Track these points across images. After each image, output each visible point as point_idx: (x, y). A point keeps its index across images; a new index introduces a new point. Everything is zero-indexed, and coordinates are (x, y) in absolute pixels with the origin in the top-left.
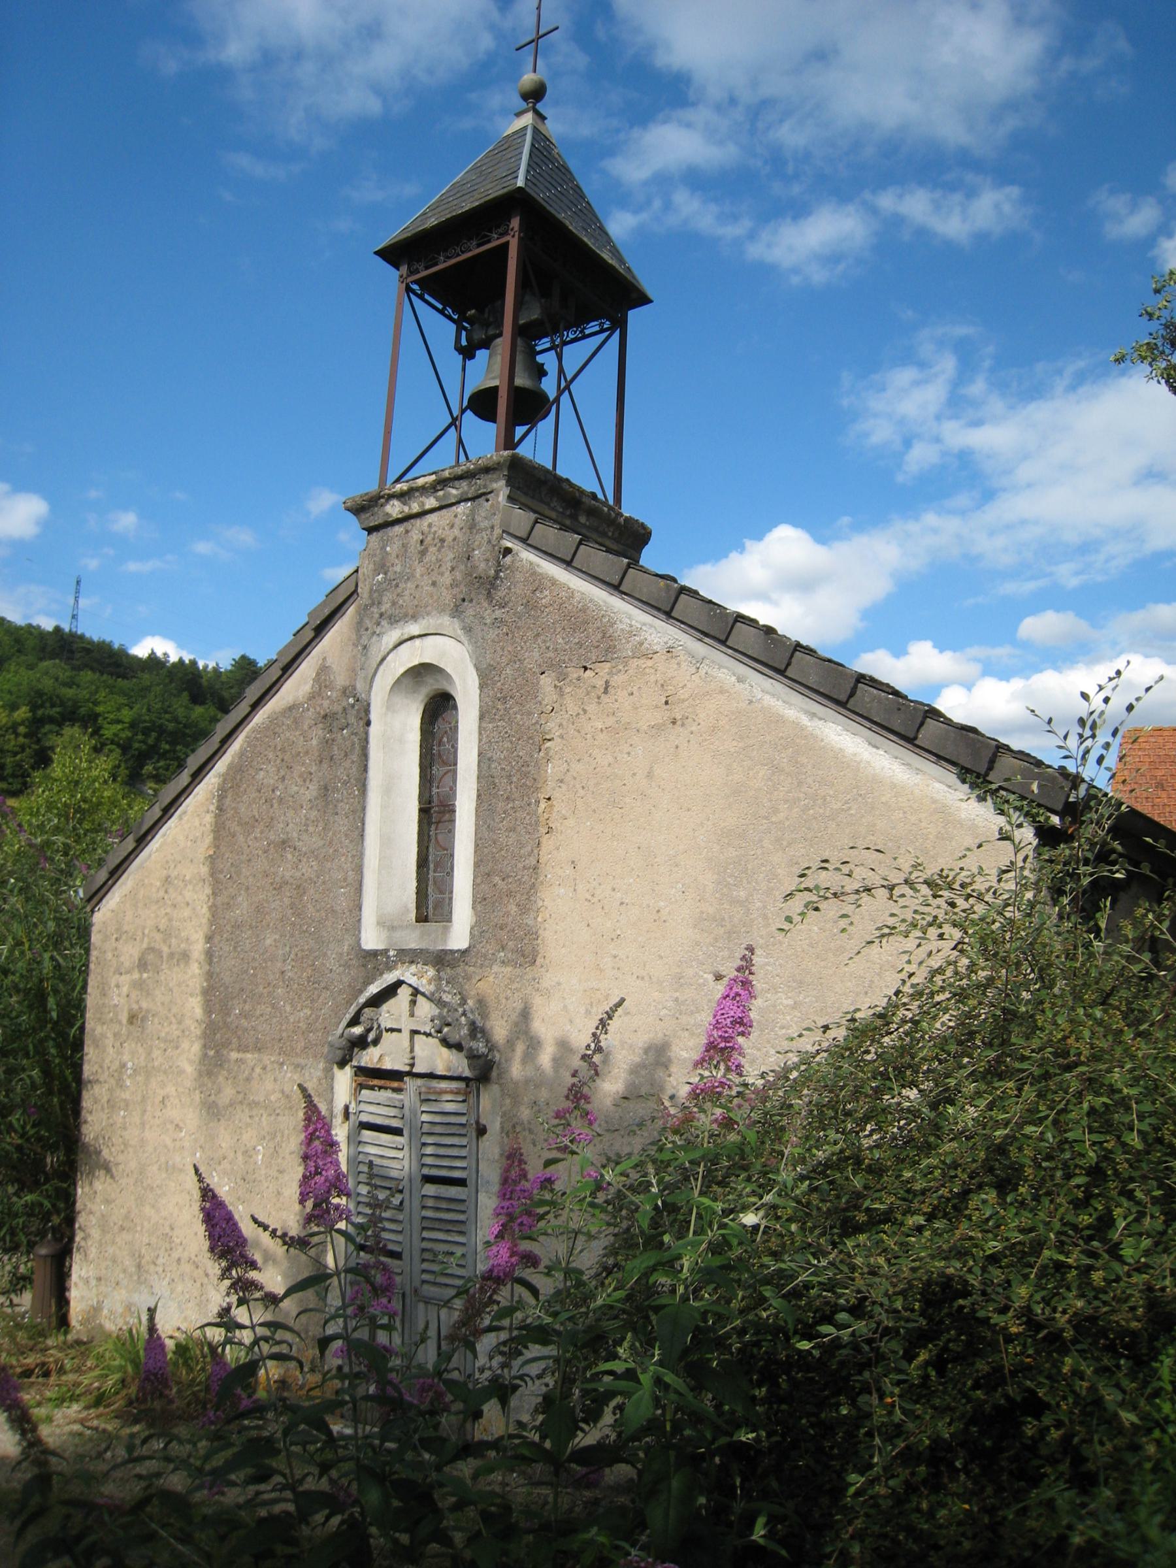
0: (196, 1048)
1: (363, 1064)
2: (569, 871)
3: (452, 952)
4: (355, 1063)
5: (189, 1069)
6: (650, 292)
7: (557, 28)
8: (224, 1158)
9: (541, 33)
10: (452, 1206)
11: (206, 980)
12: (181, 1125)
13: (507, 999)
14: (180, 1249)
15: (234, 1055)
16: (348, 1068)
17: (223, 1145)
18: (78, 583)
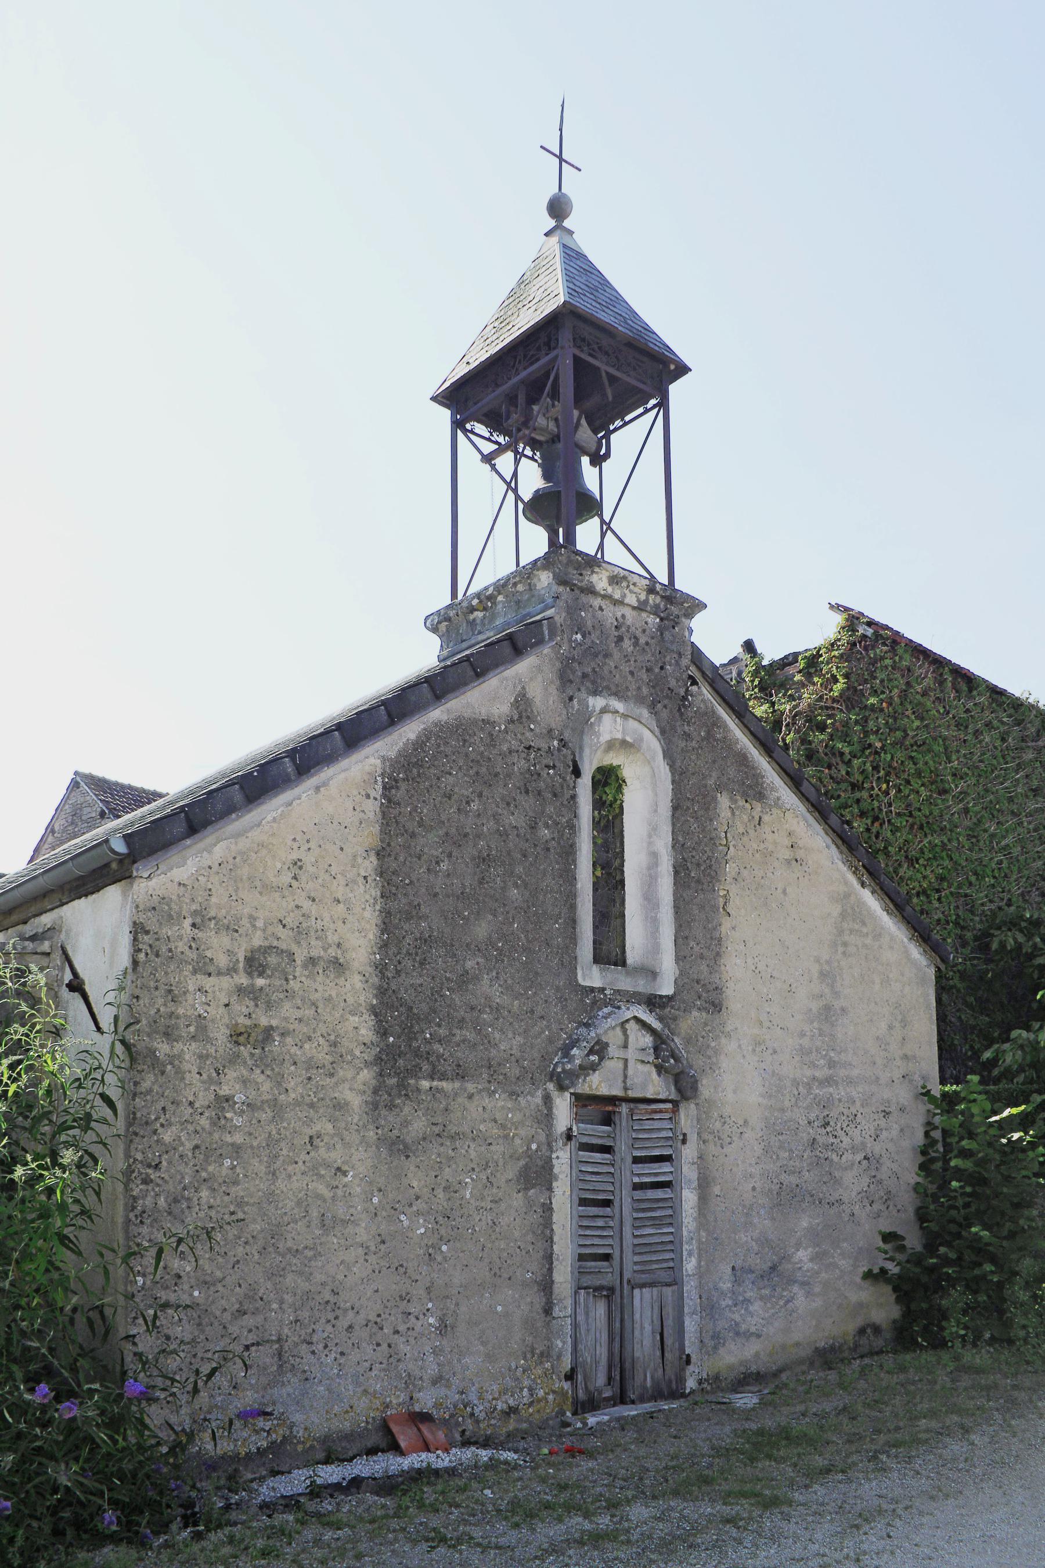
0: (366, 1075)
1: (579, 1091)
2: (742, 947)
3: (661, 997)
4: (572, 1091)
5: (356, 1101)
6: (685, 355)
7: (580, 170)
8: (417, 1198)
9: (564, 164)
10: (661, 1205)
11: (376, 996)
12: (345, 1168)
13: (703, 1037)
14: (351, 1314)
15: (425, 1084)
16: (567, 1095)
17: (415, 1184)
18: (577, 168)
